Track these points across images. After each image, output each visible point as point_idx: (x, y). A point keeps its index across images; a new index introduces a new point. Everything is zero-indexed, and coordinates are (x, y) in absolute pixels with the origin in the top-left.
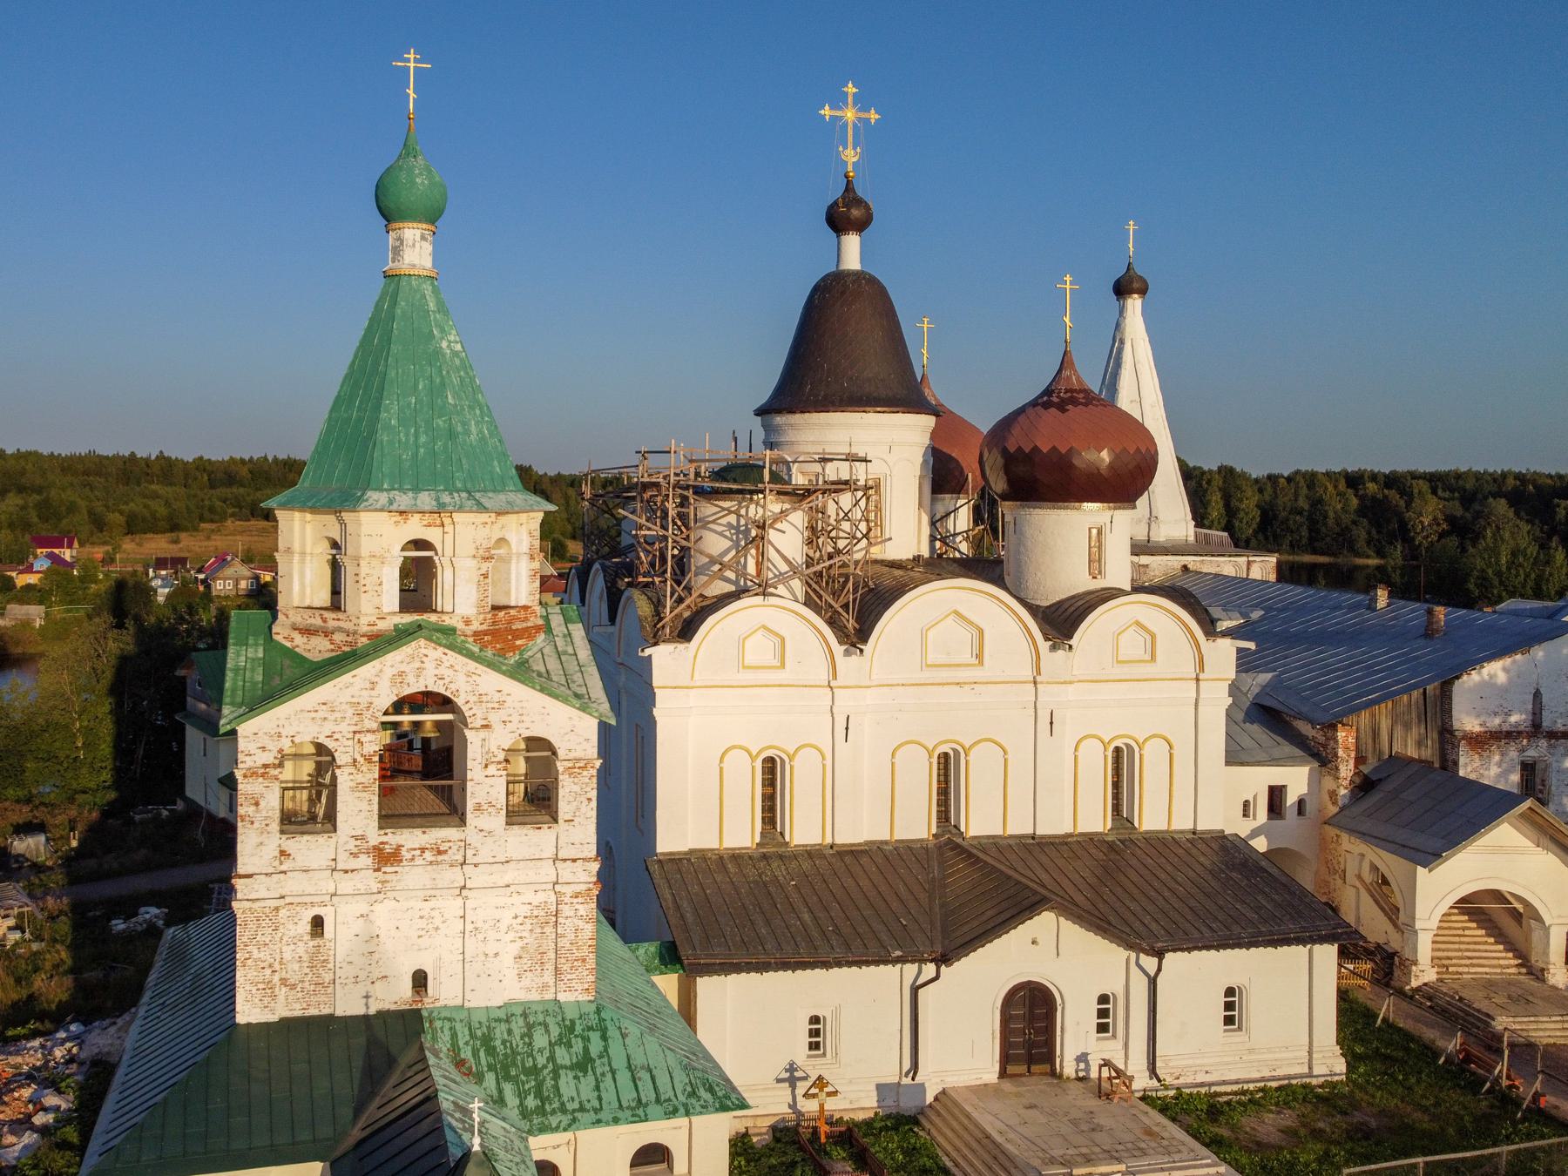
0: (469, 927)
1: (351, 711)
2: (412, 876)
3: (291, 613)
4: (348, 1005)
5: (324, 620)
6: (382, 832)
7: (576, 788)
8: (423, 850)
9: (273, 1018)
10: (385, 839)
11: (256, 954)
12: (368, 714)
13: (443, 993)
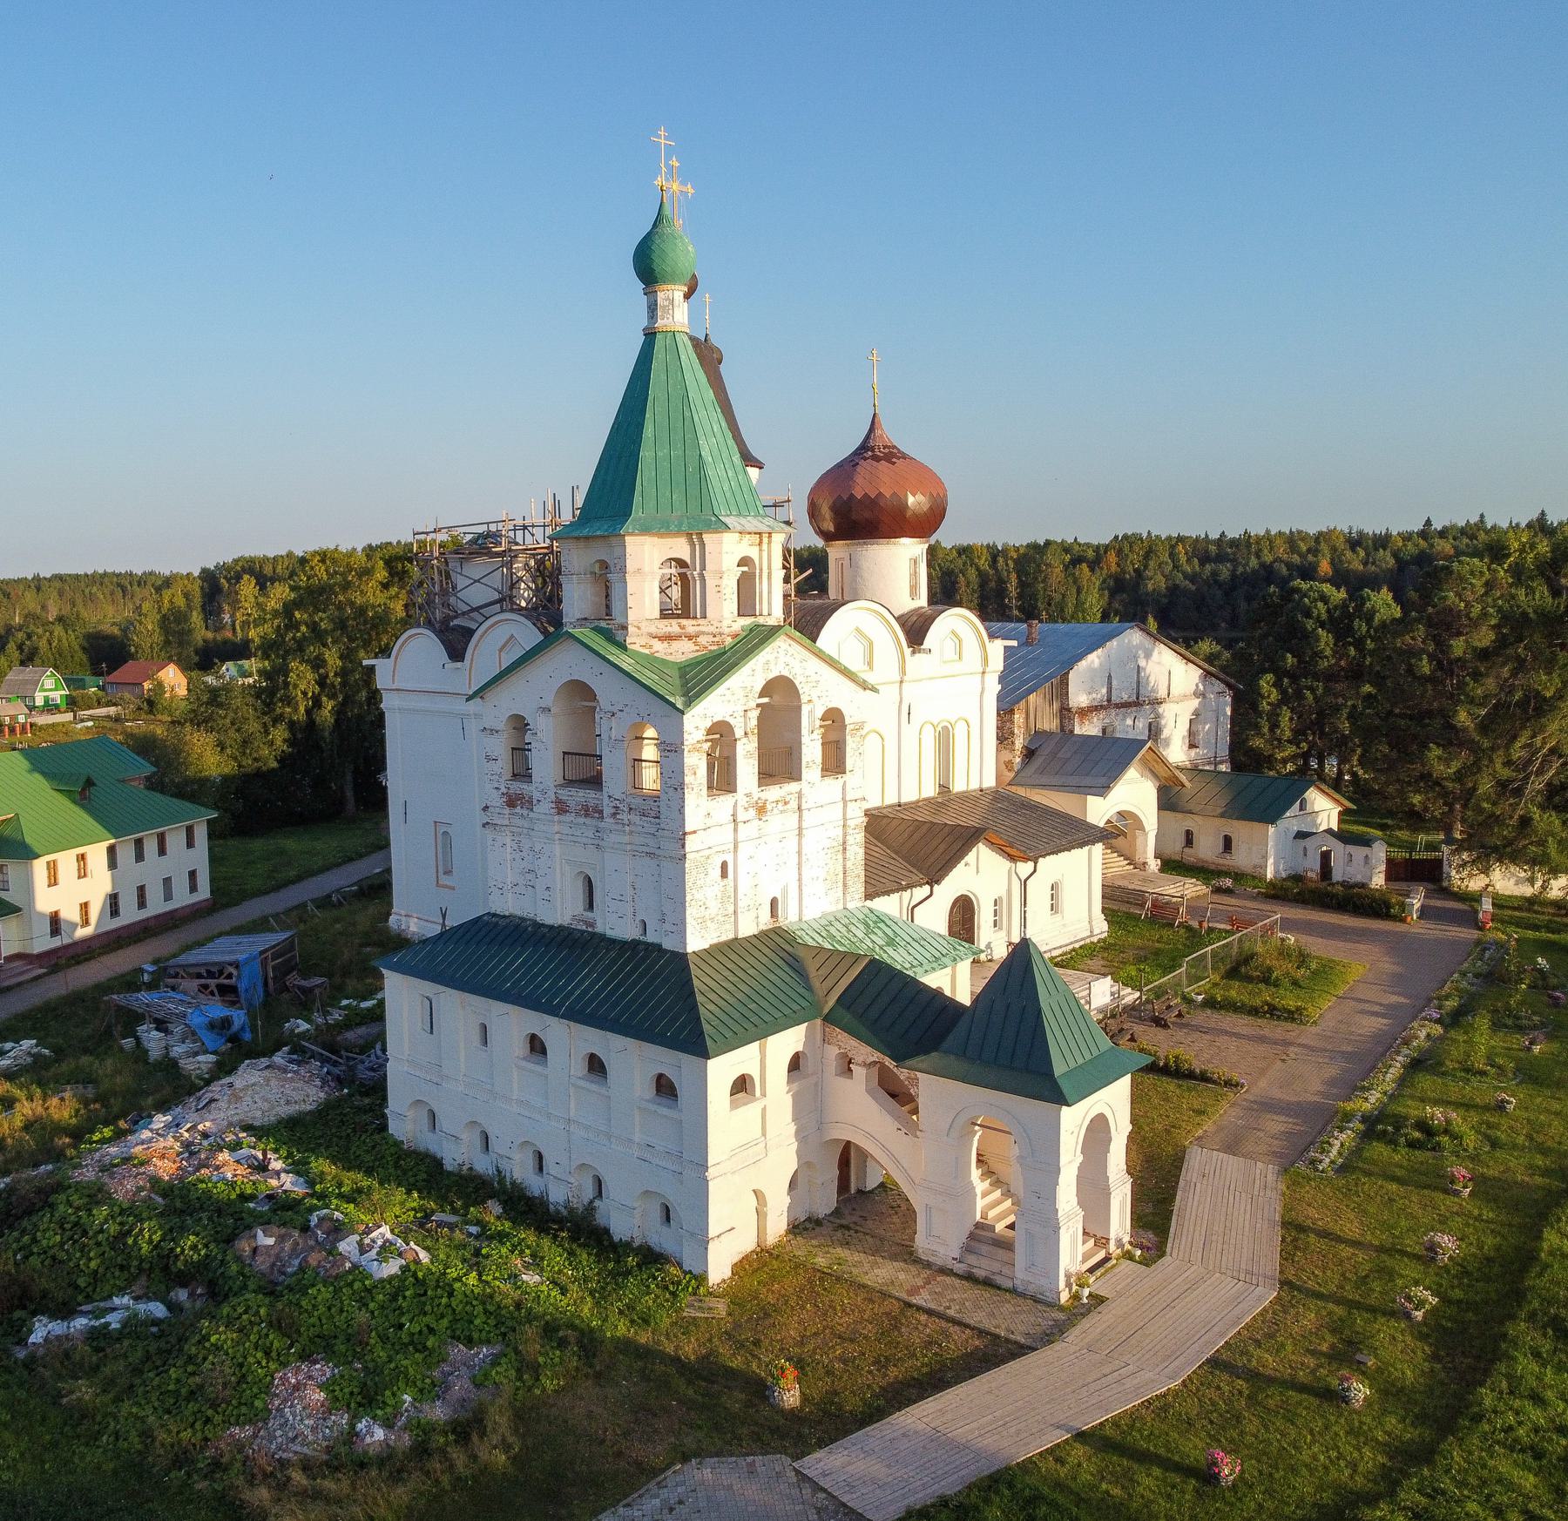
0: (804, 858)
1: (742, 693)
3: (643, 625)
4: (747, 929)
5: (682, 627)
7: (854, 746)
9: (707, 946)
11: (697, 896)
12: (750, 696)
13: (789, 917)
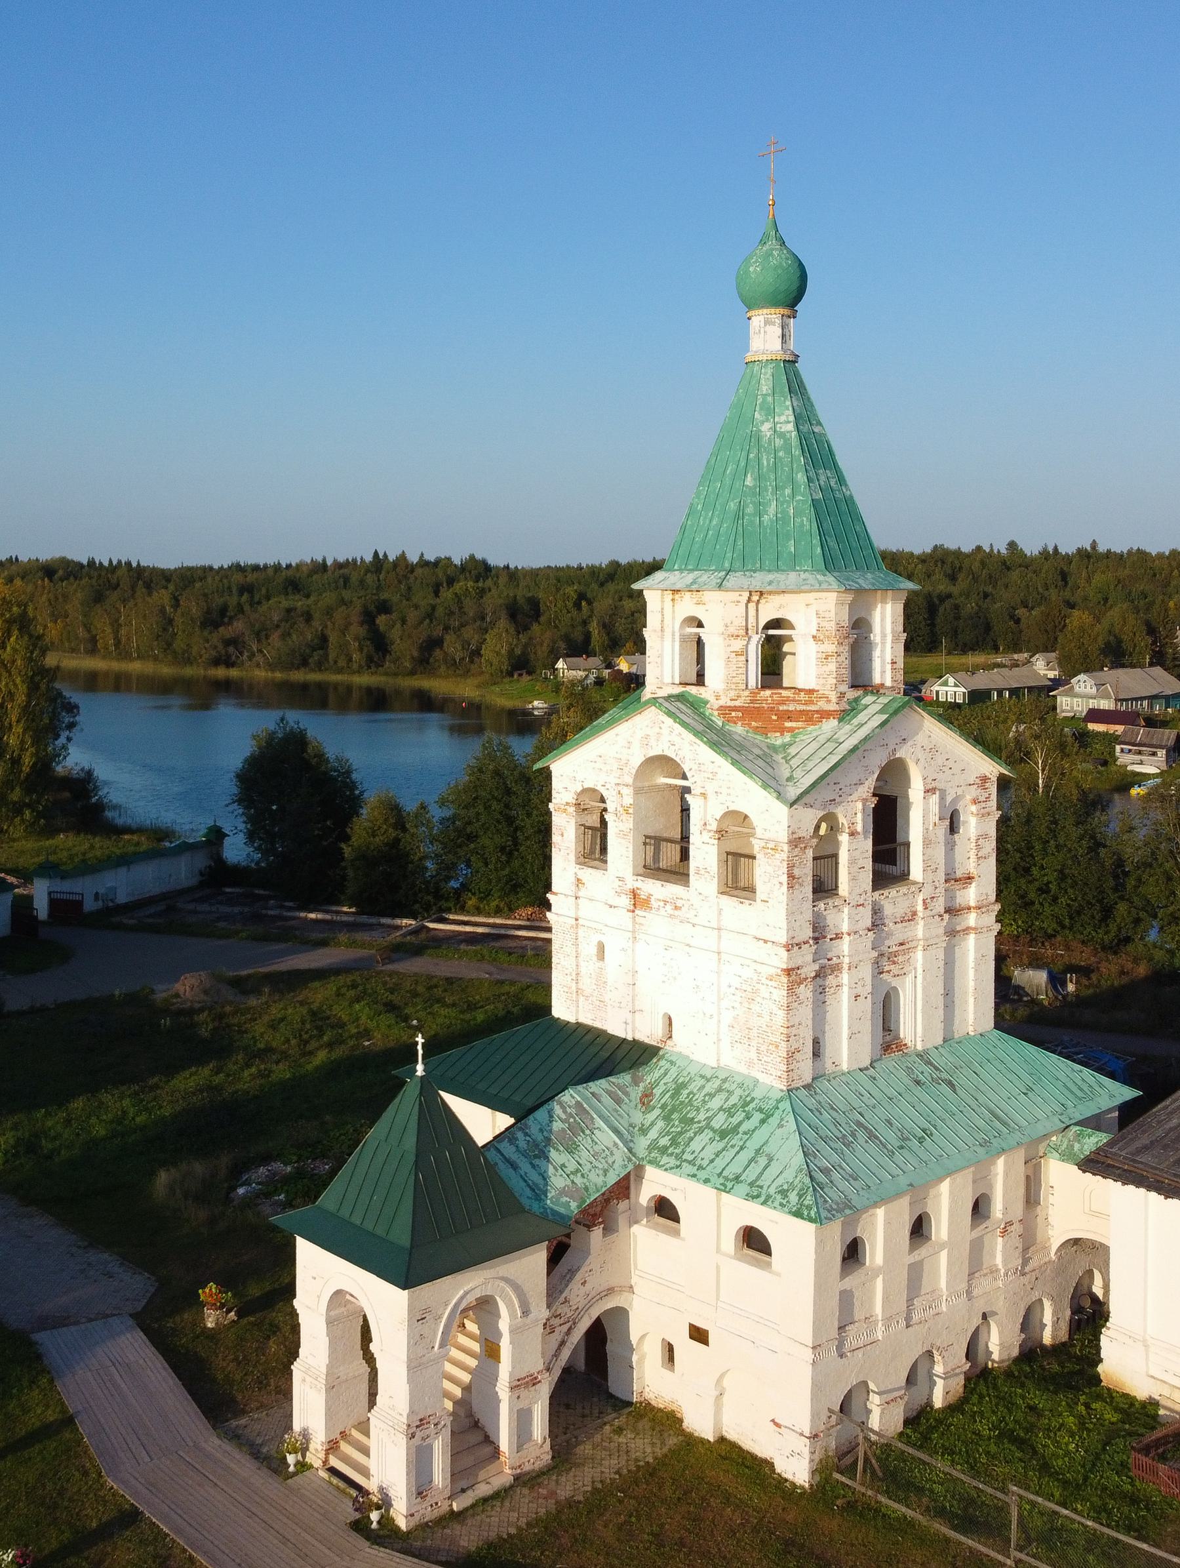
2: (655, 922)
6: (635, 878)
7: (770, 869)
8: (666, 902)
10: (639, 884)
12: (626, 770)
